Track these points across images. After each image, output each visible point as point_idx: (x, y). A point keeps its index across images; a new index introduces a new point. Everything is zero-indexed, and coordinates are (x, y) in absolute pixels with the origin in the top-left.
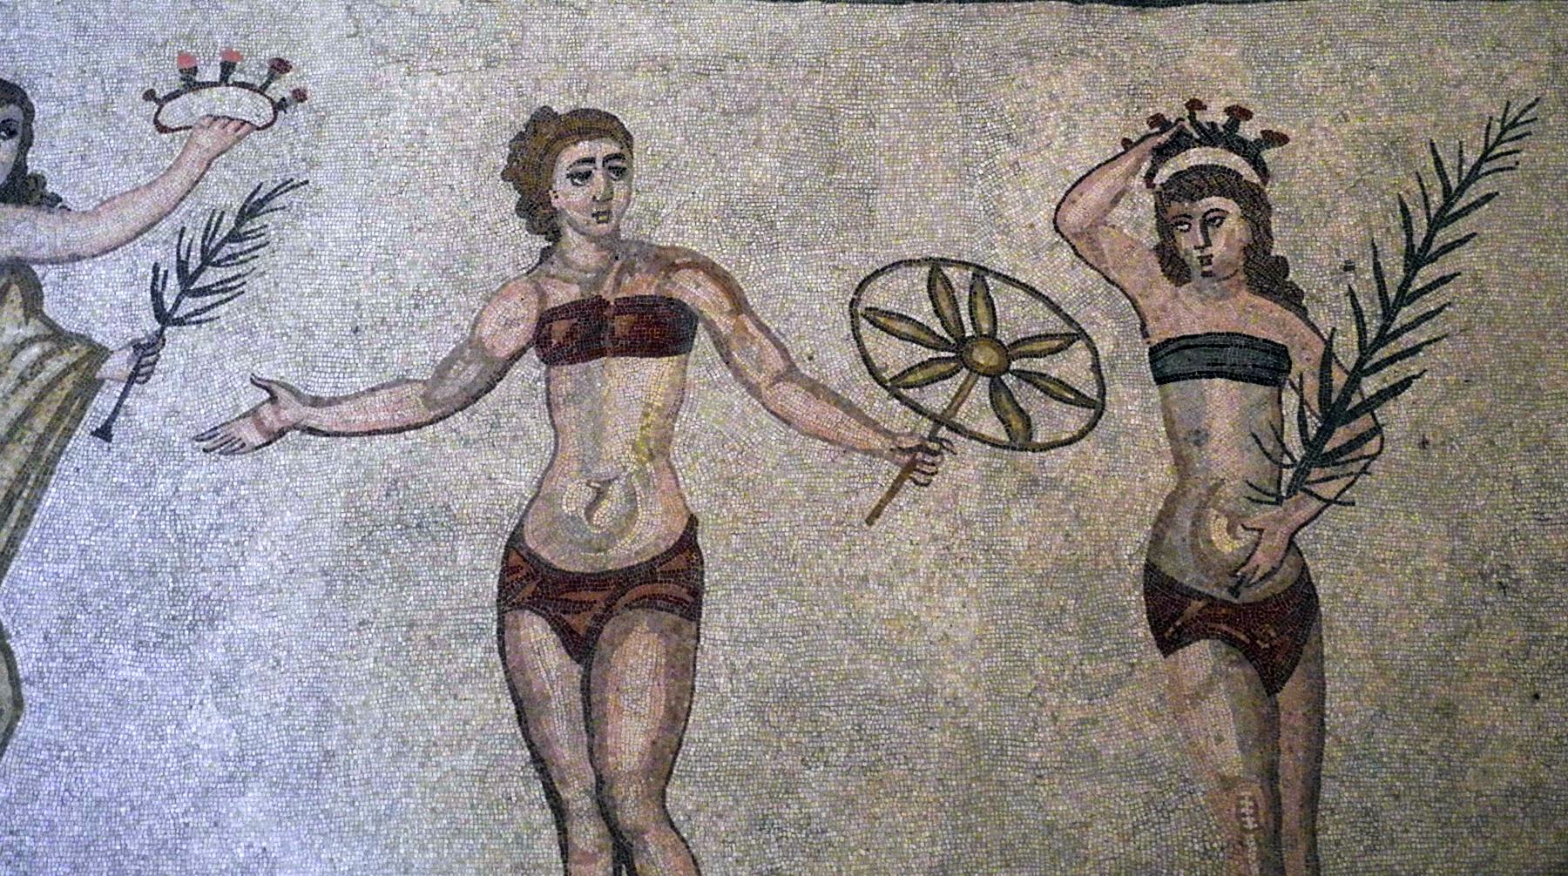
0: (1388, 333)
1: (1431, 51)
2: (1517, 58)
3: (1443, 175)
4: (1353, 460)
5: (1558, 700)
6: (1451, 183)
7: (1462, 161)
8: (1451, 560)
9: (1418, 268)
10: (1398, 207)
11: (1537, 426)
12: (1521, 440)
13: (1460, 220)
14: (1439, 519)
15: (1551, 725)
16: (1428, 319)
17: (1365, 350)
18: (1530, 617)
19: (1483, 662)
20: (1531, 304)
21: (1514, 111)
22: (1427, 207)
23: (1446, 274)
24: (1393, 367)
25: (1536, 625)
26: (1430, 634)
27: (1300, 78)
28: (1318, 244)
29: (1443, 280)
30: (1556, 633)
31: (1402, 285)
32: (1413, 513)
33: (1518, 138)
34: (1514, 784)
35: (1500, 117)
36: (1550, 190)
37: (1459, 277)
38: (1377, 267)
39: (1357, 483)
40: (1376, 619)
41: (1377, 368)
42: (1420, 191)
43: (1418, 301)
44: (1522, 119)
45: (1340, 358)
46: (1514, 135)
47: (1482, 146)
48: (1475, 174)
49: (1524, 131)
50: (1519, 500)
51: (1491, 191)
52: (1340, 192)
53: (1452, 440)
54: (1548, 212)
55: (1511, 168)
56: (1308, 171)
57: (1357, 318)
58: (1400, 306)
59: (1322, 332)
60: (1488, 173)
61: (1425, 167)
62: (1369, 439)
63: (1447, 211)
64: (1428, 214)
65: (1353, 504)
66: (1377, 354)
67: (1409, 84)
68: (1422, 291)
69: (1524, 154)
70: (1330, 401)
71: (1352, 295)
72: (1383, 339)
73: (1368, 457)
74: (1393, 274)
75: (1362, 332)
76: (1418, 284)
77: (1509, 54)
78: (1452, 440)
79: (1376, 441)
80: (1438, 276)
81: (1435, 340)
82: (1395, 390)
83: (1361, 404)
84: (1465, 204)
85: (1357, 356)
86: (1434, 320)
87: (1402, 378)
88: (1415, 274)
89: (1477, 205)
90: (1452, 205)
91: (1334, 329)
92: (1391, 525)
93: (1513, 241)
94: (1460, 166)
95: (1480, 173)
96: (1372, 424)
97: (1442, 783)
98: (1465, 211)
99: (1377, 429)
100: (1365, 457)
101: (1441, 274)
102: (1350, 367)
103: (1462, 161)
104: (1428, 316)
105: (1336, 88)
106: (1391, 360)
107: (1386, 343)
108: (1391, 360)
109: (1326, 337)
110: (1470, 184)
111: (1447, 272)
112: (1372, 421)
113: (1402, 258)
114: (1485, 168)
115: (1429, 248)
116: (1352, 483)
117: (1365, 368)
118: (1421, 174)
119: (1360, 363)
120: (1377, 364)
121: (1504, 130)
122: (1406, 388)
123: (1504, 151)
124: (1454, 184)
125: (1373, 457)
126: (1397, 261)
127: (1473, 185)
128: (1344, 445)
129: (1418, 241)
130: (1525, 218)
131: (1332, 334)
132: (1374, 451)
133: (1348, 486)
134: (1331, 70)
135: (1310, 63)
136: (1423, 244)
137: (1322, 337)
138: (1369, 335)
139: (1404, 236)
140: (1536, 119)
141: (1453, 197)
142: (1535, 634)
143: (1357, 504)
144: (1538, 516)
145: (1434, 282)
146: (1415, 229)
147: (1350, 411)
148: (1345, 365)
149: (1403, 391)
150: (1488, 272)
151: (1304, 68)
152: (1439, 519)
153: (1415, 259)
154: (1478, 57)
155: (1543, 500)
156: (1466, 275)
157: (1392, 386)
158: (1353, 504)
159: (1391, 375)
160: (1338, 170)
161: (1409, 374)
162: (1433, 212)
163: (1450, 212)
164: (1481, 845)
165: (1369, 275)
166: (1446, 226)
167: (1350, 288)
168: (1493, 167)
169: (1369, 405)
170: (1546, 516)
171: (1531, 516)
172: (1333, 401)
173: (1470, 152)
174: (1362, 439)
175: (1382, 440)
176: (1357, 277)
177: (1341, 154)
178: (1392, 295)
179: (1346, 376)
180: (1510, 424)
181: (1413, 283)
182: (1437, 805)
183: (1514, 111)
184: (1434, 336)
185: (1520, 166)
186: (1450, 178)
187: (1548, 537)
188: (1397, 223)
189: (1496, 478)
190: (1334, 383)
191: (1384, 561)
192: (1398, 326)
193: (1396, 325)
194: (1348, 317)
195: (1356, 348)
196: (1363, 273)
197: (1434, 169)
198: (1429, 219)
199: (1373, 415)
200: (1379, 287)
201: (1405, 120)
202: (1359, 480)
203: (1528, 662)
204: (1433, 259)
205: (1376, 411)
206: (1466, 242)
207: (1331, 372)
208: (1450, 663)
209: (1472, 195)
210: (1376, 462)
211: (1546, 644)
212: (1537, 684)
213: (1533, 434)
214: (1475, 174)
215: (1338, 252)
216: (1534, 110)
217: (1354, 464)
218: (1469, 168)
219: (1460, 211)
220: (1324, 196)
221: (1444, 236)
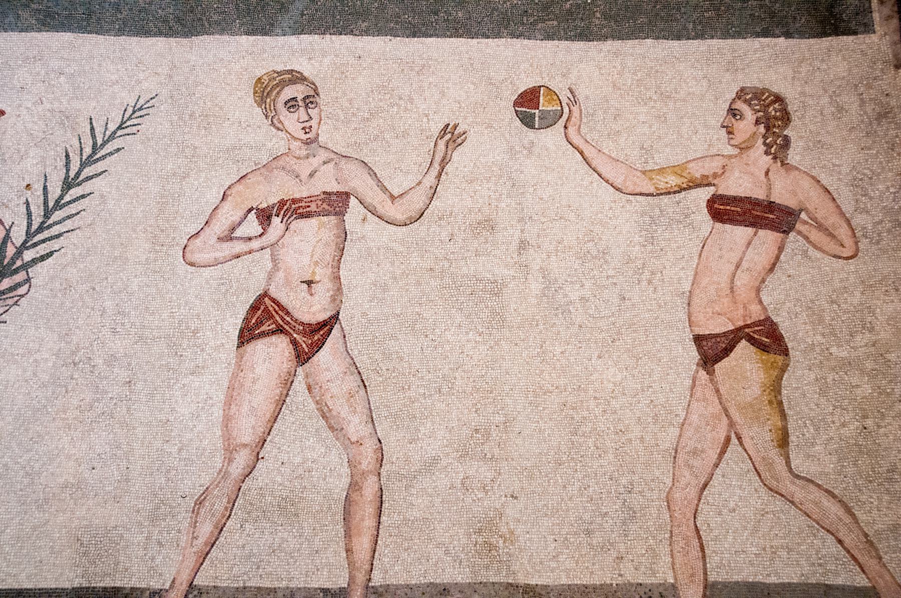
0: (45, 225)
1: (100, 65)
2: (149, 71)
3: (93, 136)
4: (10, 298)
5: (104, 433)
6: (98, 141)
7: (106, 129)
8: (57, 355)
9: (69, 190)
10: (64, 154)
11: (122, 280)
12: (111, 287)
13: (99, 163)
14: (55, 331)
15: (97, 447)
16: (70, 218)
17: (29, 235)
18: (97, 387)
19: (65, 412)
20: (131, 211)
21: (141, 102)
22: (81, 154)
23: (85, 193)
24: (44, 245)
25: (100, 391)
26: (37, 396)
27: (19, 77)
28: (13, 174)
29: (83, 197)
30: (110, 396)
31: (58, 199)
32: (40, 328)
33: (141, 116)
34: (69, 481)
35: (133, 105)
36: (155, 147)
37: (92, 195)
38: (45, 188)
39: (9, 311)
40: (6, 388)
41: (35, 245)
42: (79, 145)
43: (66, 208)
44: (145, 106)
45: (13, 240)
46: (139, 115)
47: (120, 120)
48: (113, 136)
49: (146, 113)
50: (104, 321)
51: (120, 147)
52: (31, 145)
53: (71, 286)
54: (151, 158)
55: (134, 134)
56: (14, 132)
57: (28, 216)
58: (55, 210)
59: (5, 224)
60: (119, 137)
61: (84, 132)
62: (23, 286)
63: (92, 157)
64: (81, 159)
65: (6, 322)
66: (36, 237)
67: (83, 83)
68: (69, 203)
69: (143, 126)
70: (3, 263)
71: (27, 203)
72: (40, 229)
73: (20, 296)
74: (54, 193)
75: (29, 225)
76: (67, 198)
77: (145, 69)
78: (71, 286)
79: (27, 286)
80: (80, 194)
81: (72, 230)
82: (43, 258)
83: (21, 265)
84: (104, 154)
85: (24, 239)
86: (73, 219)
87: (48, 251)
88: (66, 193)
89: (110, 154)
90: (96, 154)
91: (13, 223)
92: (25, 335)
93: (128, 175)
94: (105, 132)
95: (116, 136)
96: (26, 277)
97: (26, 481)
98: (104, 157)
99: (28, 280)
100: (18, 296)
101: (82, 193)
102: (18, 245)
103: (106, 129)
104: (69, 217)
105: (39, 84)
106: (43, 241)
107: (43, 231)
108: (43, 241)
109: (8, 227)
110: (109, 142)
111: (87, 191)
112: (26, 276)
113: (61, 183)
114: (119, 133)
115: (78, 178)
116: (7, 311)
117: (27, 245)
118: (81, 136)
119: (25, 242)
120: (35, 243)
121: (134, 112)
122: (50, 257)
123: (132, 124)
124: (100, 141)
125: (22, 296)
126: (58, 185)
127: (111, 143)
128: (7, 289)
129: (72, 174)
130: (137, 162)
131: (12, 225)
132: (23, 293)
133: (4, 312)
134: (38, 74)
135: (26, 69)
136: (75, 175)
137: (5, 227)
138: (33, 227)
139: (65, 171)
140: (154, 106)
141: (97, 149)
142: (98, 396)
143: (8, 322)
144: (113, 330)
145: (77, 197)
146: (72, 167)
147: (14, 270)
148: (16, 244)
149: (47, 258)
150: (110, 193)
151: (22, 72)
152: (55, 331)
153: (68, 185)
154: (126, 70)
155: (117, 321)
156: (97, 194)
157: (42, 256)
158: (6, 322)
159: (42, 250)
160: (32, 132)
161: (53, 250)
162: (84, 158)
163: (94, 158)
164: (42, 515)
165: (40, 192)
166: (90, 166)
167: (27, 200)
168: (124, 133)
169: (26, 266)
170: (117, 330)
171: (109, 330)
172: (5, 263)
173: (112, 124)
174: (18, 285)
175: (30, 286)
176: (32, 194)
177: (36, 123)
178: (51, 204)
179: (15, 250)
180: (107, 278)
181: (65, 198)
182: (21, 493)
183: (141, 102)
184: (72, 228)
185: (139, 133)
186: (98, 139)
187: (116, 342)
188: (61, 163)
189: (93, 309)
190: (7, 253)
191: (18, 354)
192: (52, 222)
193: (50, 221)
194: (23, 216)
195: (24, 234)
196: (36, 192)
197: (89, 133)
198: (81, 161)
199: (27, 272)
200: (45, 199)
201: (76, 104)
202: (12, 309)
203: (91, 411)
204: (79, 184)
205: (29, 270)
206: (100, 175)
207: (6, 247)
208: (45, 412)
209: (109, 148)
210: (24, 298)
211: (104, 401)
212: (94, 424)
213: (119, 284)
214: (113, 136)
215: (23, 179)
216: (154, 100)
217: (11, 300)
218: (110, 133)
219: (100, 158)
220: (21, 147)
221: (88, 171)
